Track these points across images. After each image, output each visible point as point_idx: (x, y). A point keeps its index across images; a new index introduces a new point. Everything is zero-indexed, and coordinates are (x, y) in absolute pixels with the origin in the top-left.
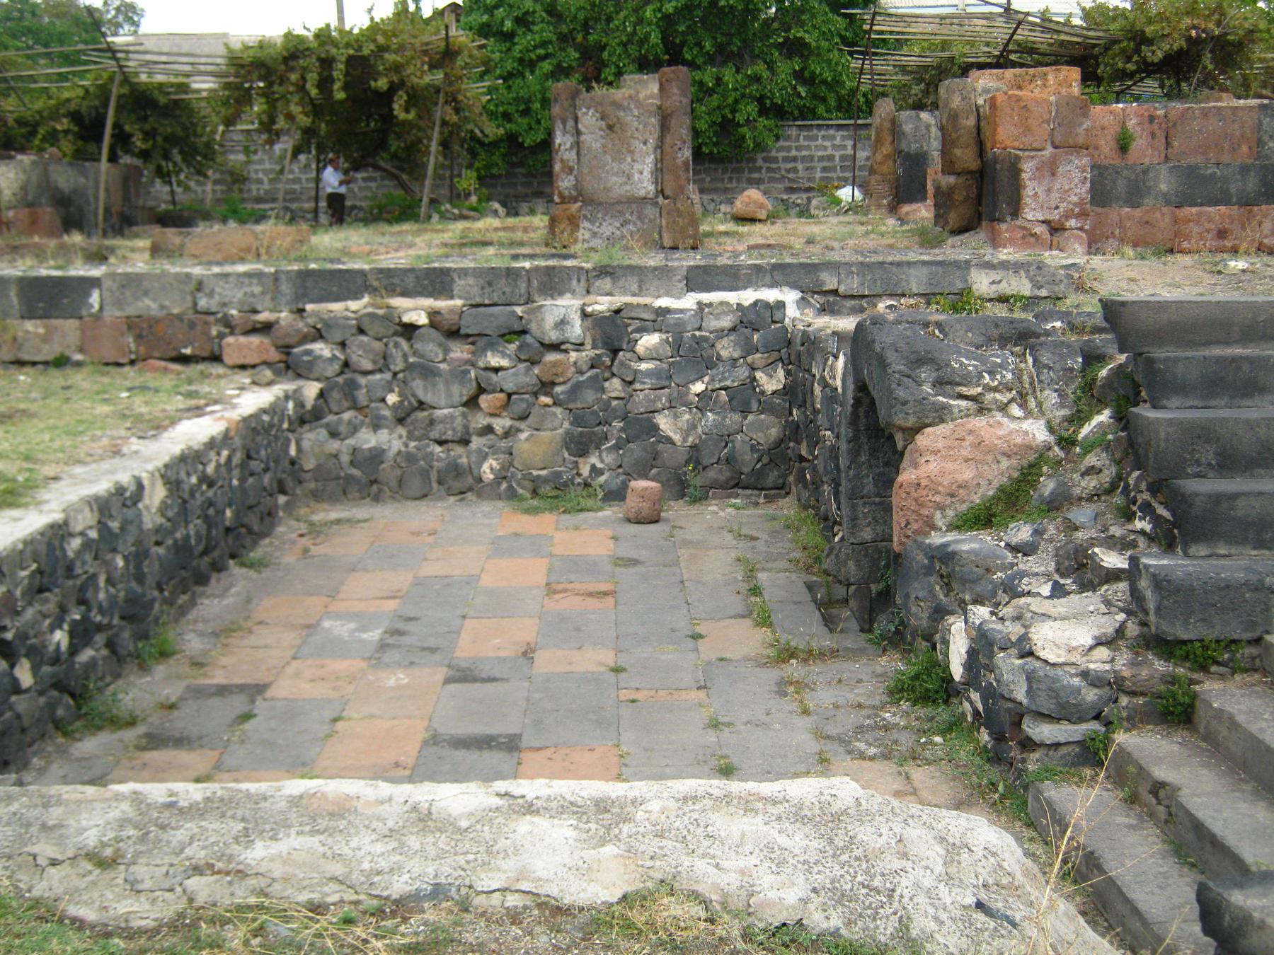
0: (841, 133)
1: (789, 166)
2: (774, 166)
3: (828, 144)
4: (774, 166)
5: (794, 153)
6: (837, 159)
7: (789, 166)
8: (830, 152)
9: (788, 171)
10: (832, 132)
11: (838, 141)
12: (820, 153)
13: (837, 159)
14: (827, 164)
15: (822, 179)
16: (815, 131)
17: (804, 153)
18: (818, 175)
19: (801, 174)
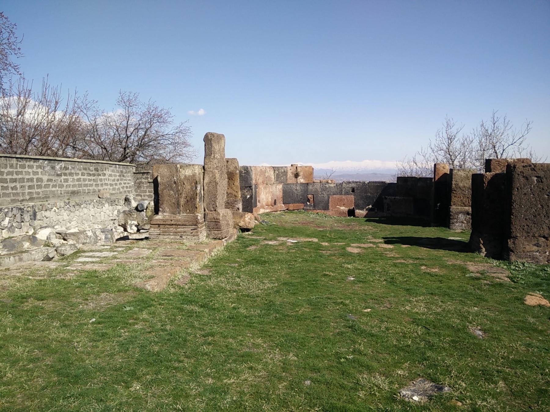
0: (35, 164)
1: (13, 185)
2: (5, 185)
3: (30, 170)
4: (5, 185)
5: (15, 176)
6: (35, 180)
7: (13, 185)
8: (31, 176)
9: (12, 189)
10: (32, 163)
11: (35, 169)
12: (27, 177)
13: (35, 180)
14: (30, 184)
15: (30, 193)
16: (25, 162)
17: (20, 176)
18: (27, 191)
19: (19, 191)
